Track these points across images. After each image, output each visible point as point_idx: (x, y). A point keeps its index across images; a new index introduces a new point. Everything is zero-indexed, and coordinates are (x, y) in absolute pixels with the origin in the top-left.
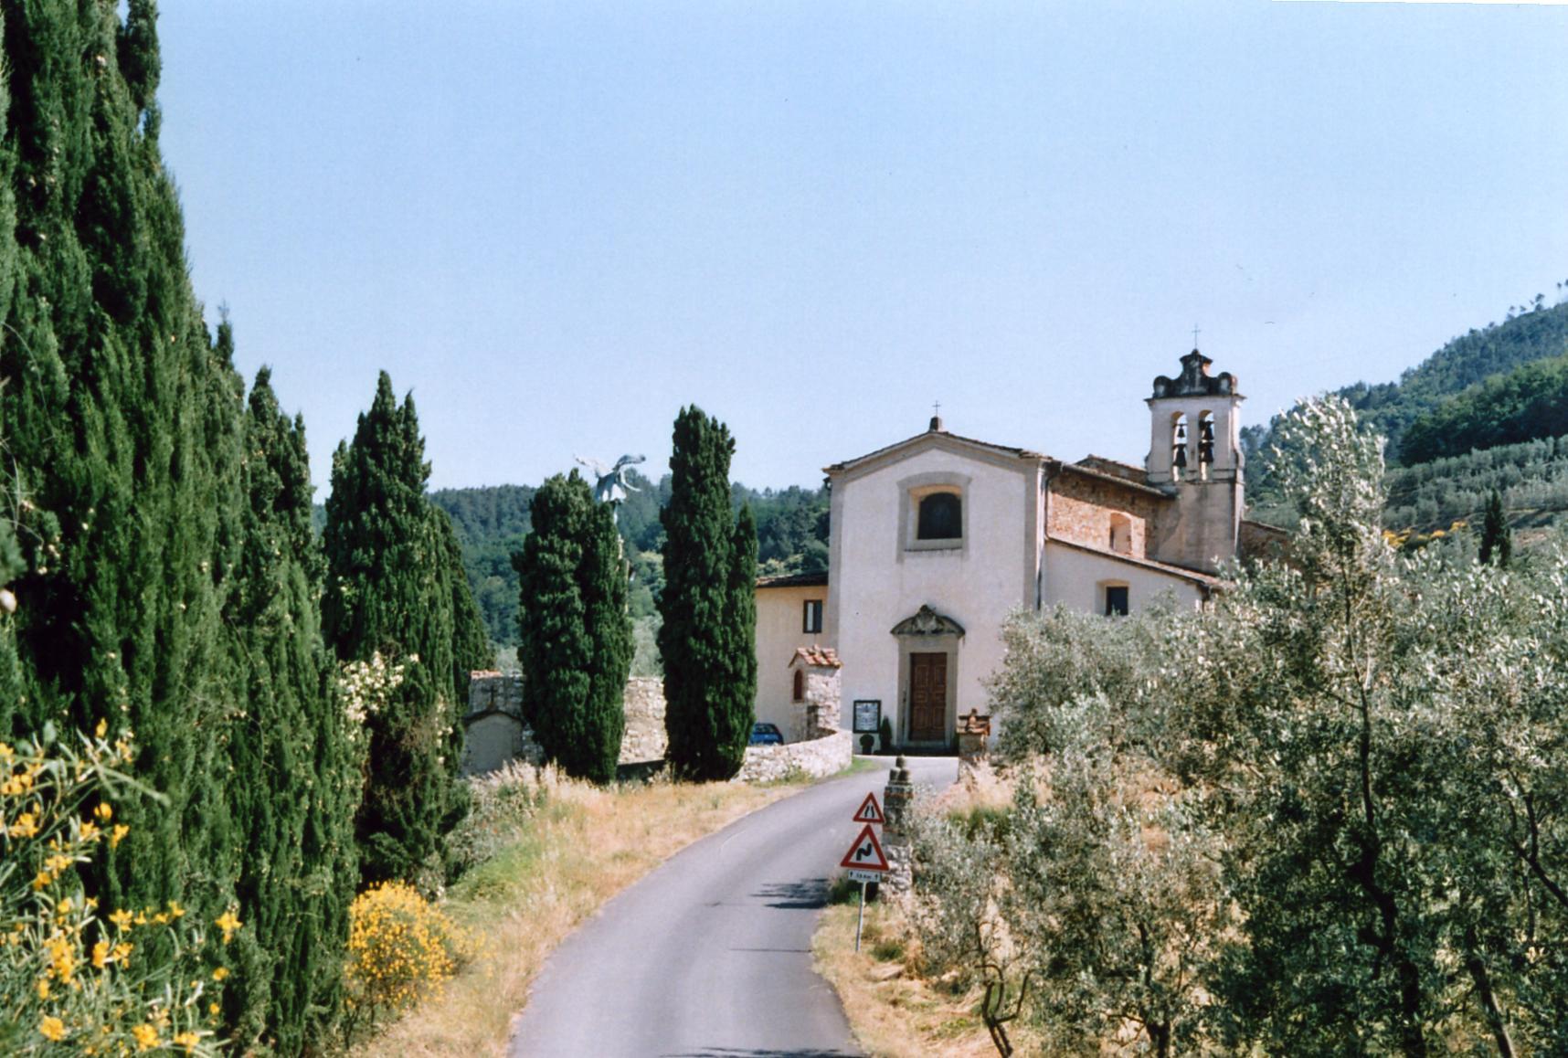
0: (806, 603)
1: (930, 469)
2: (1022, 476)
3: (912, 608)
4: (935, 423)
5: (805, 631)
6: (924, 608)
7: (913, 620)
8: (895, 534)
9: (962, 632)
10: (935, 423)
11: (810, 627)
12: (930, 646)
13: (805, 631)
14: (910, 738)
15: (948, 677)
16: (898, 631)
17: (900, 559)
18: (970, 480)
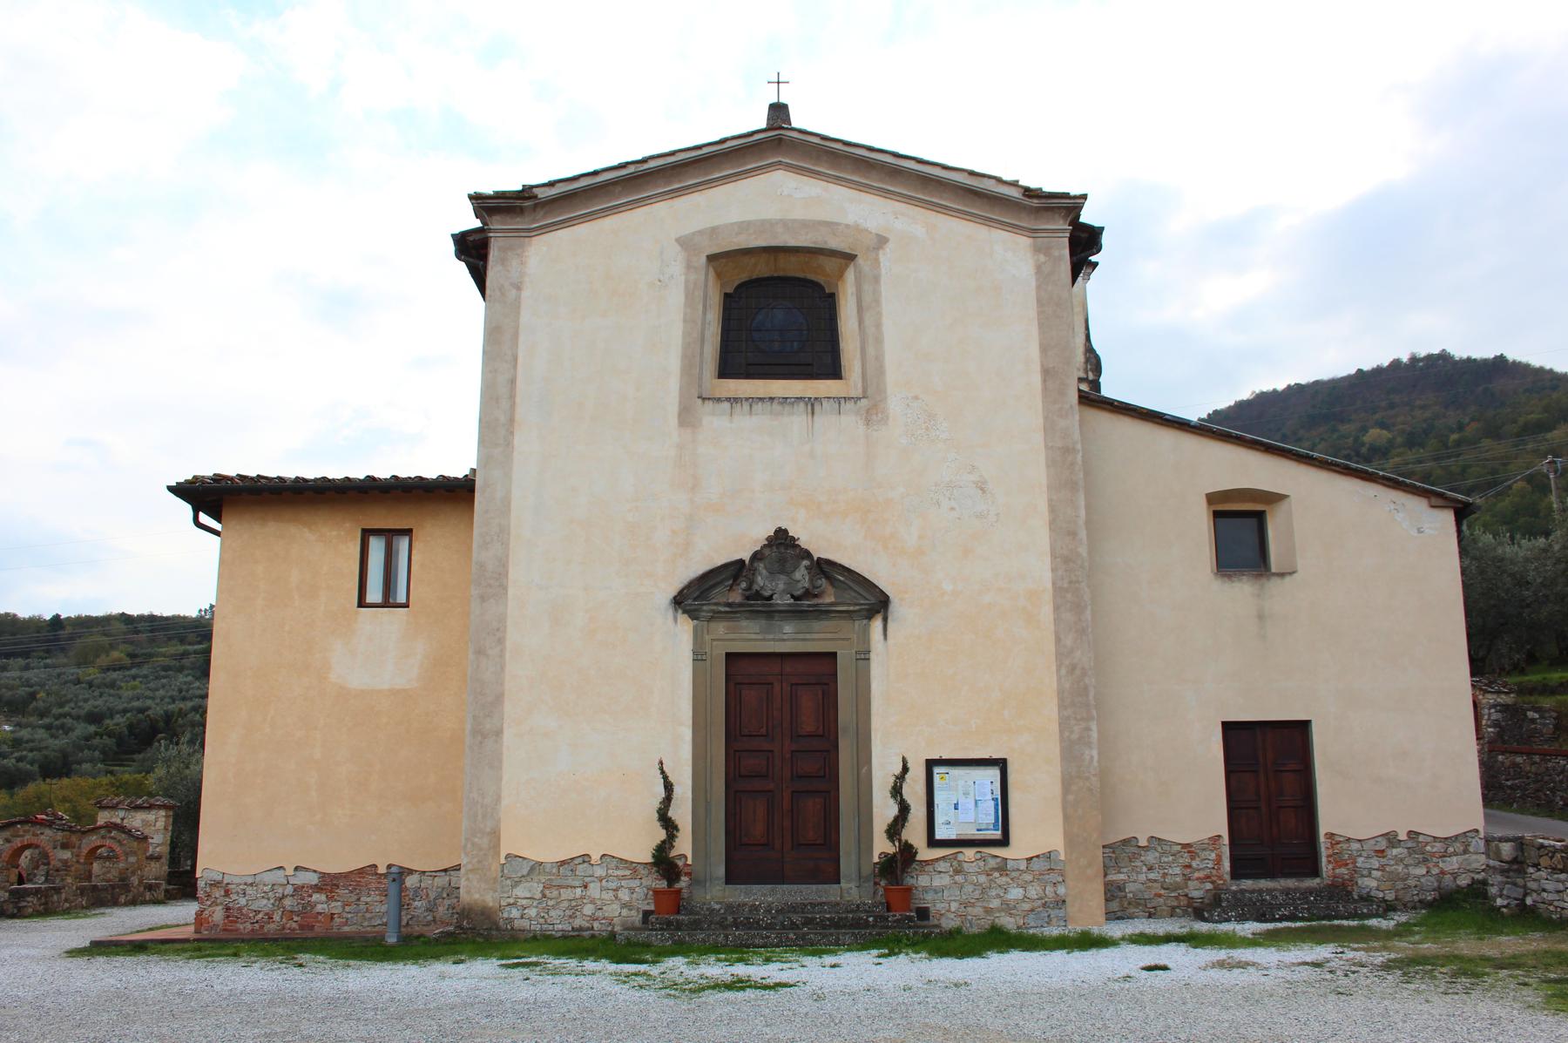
0: (367, 534)
1: (771, 212)
2: (1024, 241)
3: (739, 538)
4: (779, 111)
5: (362, 603)
6: (781, 541)
7: (735, 570)
8: (674, 362)
9: (878, 604)
10: (779, 111)
11: (374, 594)
12: (788, 638)
13: (362, 603)
14: (731, 878)
15: (845, 714)
16: (693, 599)
17: (686, 417)
18: (882, 241)
